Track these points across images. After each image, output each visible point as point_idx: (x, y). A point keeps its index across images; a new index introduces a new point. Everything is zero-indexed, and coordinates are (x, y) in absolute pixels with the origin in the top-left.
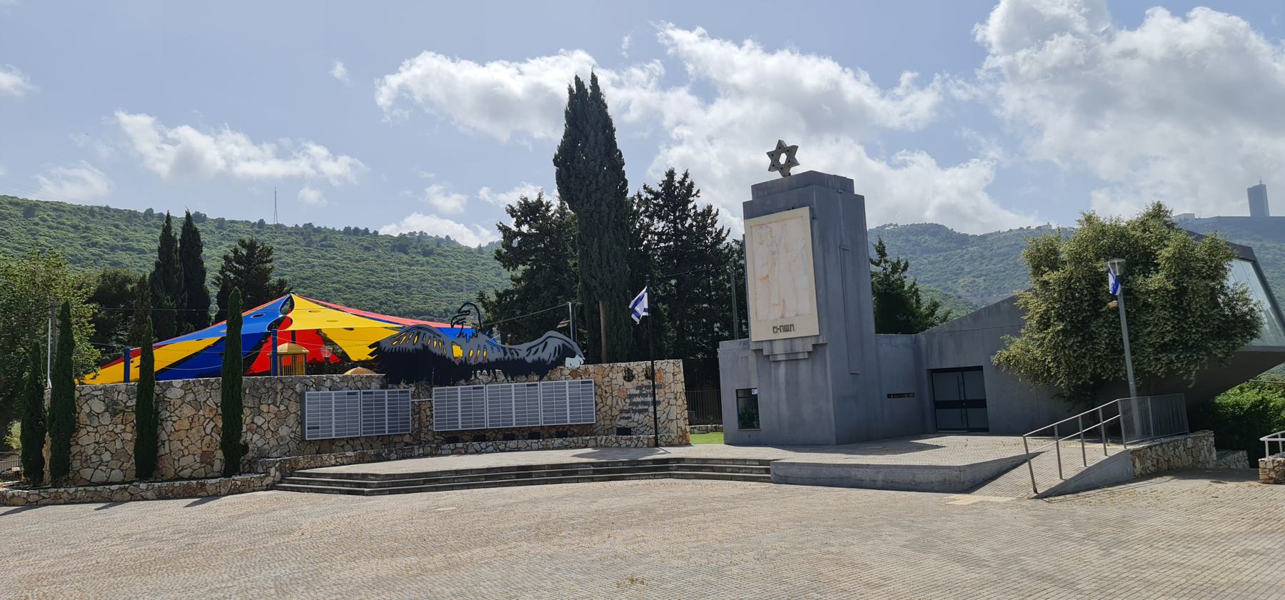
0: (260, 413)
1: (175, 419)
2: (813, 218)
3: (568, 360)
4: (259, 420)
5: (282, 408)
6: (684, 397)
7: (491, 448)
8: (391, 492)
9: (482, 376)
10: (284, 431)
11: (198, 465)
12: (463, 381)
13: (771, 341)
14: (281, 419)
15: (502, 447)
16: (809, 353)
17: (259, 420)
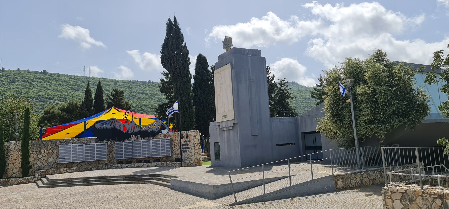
0: (40, 153)
1: (12, 155)
2: (232, 68)
3: (163, 131)
4: (40, 156)
6: (199, 145)
7: (130, 166)
9: (133, 138)
10: (51, 160)
11: (18, 173)
12: (126, 140)
13: (222, 122)
14: (50, 155)
15: (133, 166)
16: (233, 127)
17: (40, 156)
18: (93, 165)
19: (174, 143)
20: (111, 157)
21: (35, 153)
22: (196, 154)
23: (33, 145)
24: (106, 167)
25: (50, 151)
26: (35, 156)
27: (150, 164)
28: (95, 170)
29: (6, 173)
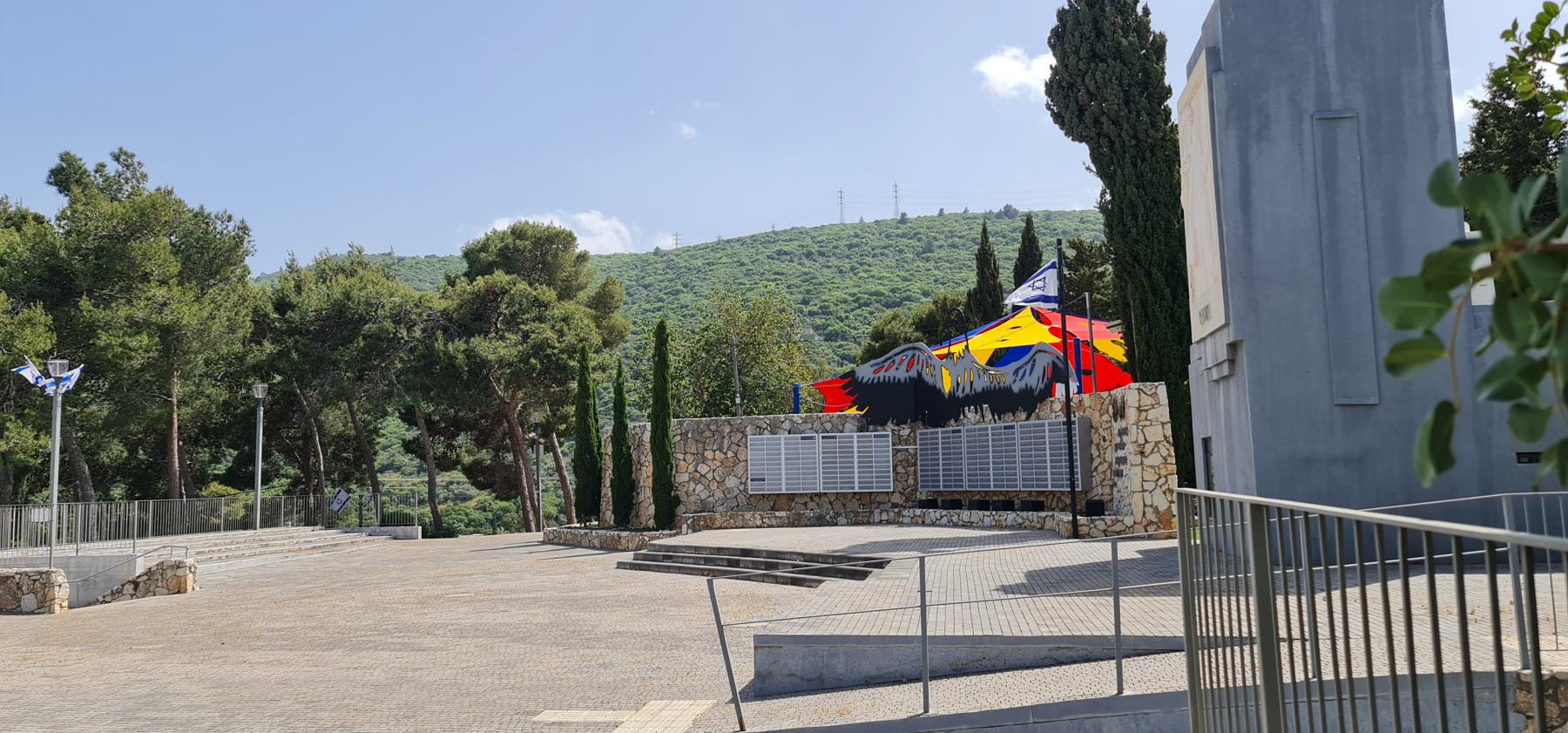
4: (703, 469)
5: (730, 454)
7: (944, 520)
8: (659, 569)
9: (970, 415)
10: (731, 482)
14: (730, 467)
15: (955, 519)
17: (703, 469)
18: (853, 505)
19: (1095, 438)
20: (911, 481)
21: (690, 458)
22: (1147, 486)
23: (684, 435)
24: (884, 517)
25: (730, 454)
26: (691, 468)
27: (955, 515)
28: (848, 524)
29: (637, 516)
